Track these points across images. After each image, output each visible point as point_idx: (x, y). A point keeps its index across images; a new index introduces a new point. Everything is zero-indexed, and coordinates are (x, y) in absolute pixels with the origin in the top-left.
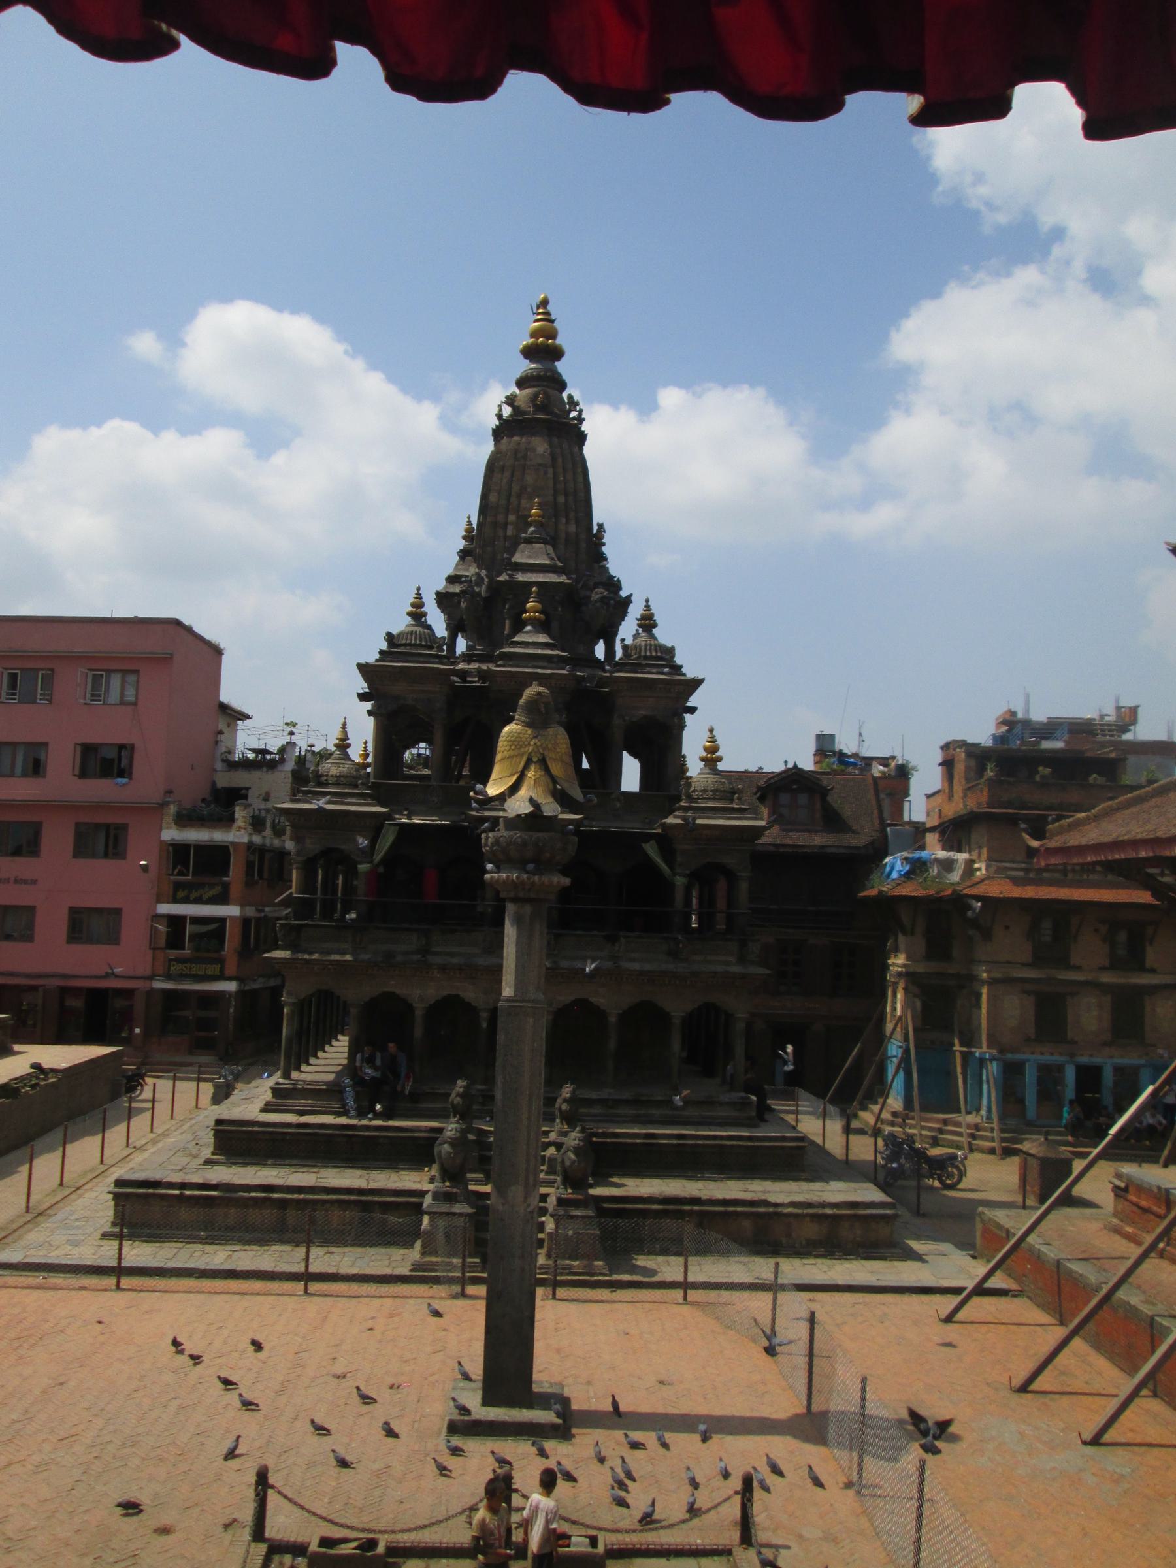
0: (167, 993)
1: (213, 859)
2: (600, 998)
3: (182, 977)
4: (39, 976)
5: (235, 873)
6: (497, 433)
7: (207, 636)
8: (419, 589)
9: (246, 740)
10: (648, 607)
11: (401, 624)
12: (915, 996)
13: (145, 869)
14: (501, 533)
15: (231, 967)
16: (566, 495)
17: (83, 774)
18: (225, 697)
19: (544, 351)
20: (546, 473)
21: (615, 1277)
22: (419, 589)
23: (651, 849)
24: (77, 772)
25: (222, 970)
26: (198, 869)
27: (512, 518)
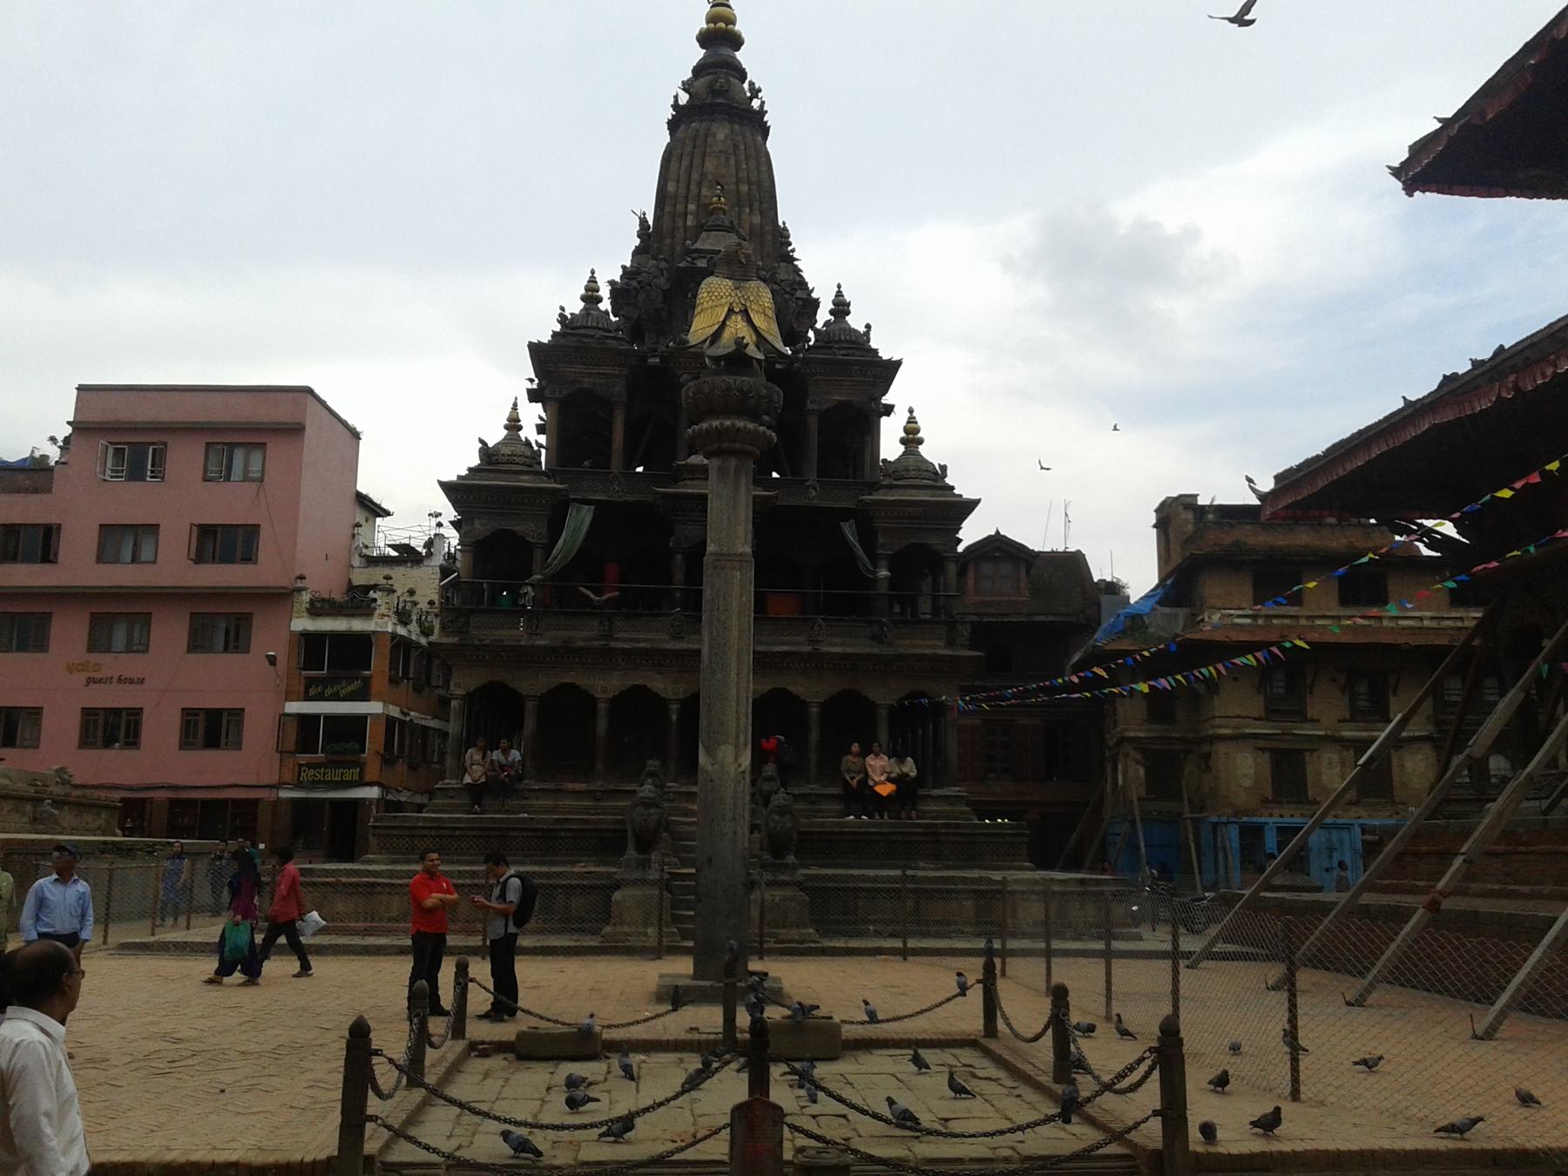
0: (295, 802)
1: (354, 649)
2: (800, 687)
3: (314, 785)
4: (147, 788)
5: (379, 663)
6: (673, 125)
7: (344, 417)
8: (593, 272)
9: (385, 535)
10: (839, 294)
11: (575, 307)
12: (1138, 762)
13: (272, 661)
14: (680, 223)
15: (373, 770)
16: (749, 184)
17: (199, 559)
18: (363, 486)
19: (720, 38)
20: (727, 160)
21: (828, 943)
22: (593, 272)
23: (849, 530)
24: (193, 556)
25: (361, 774)
26: (334, 660)
27: (692, 207)
